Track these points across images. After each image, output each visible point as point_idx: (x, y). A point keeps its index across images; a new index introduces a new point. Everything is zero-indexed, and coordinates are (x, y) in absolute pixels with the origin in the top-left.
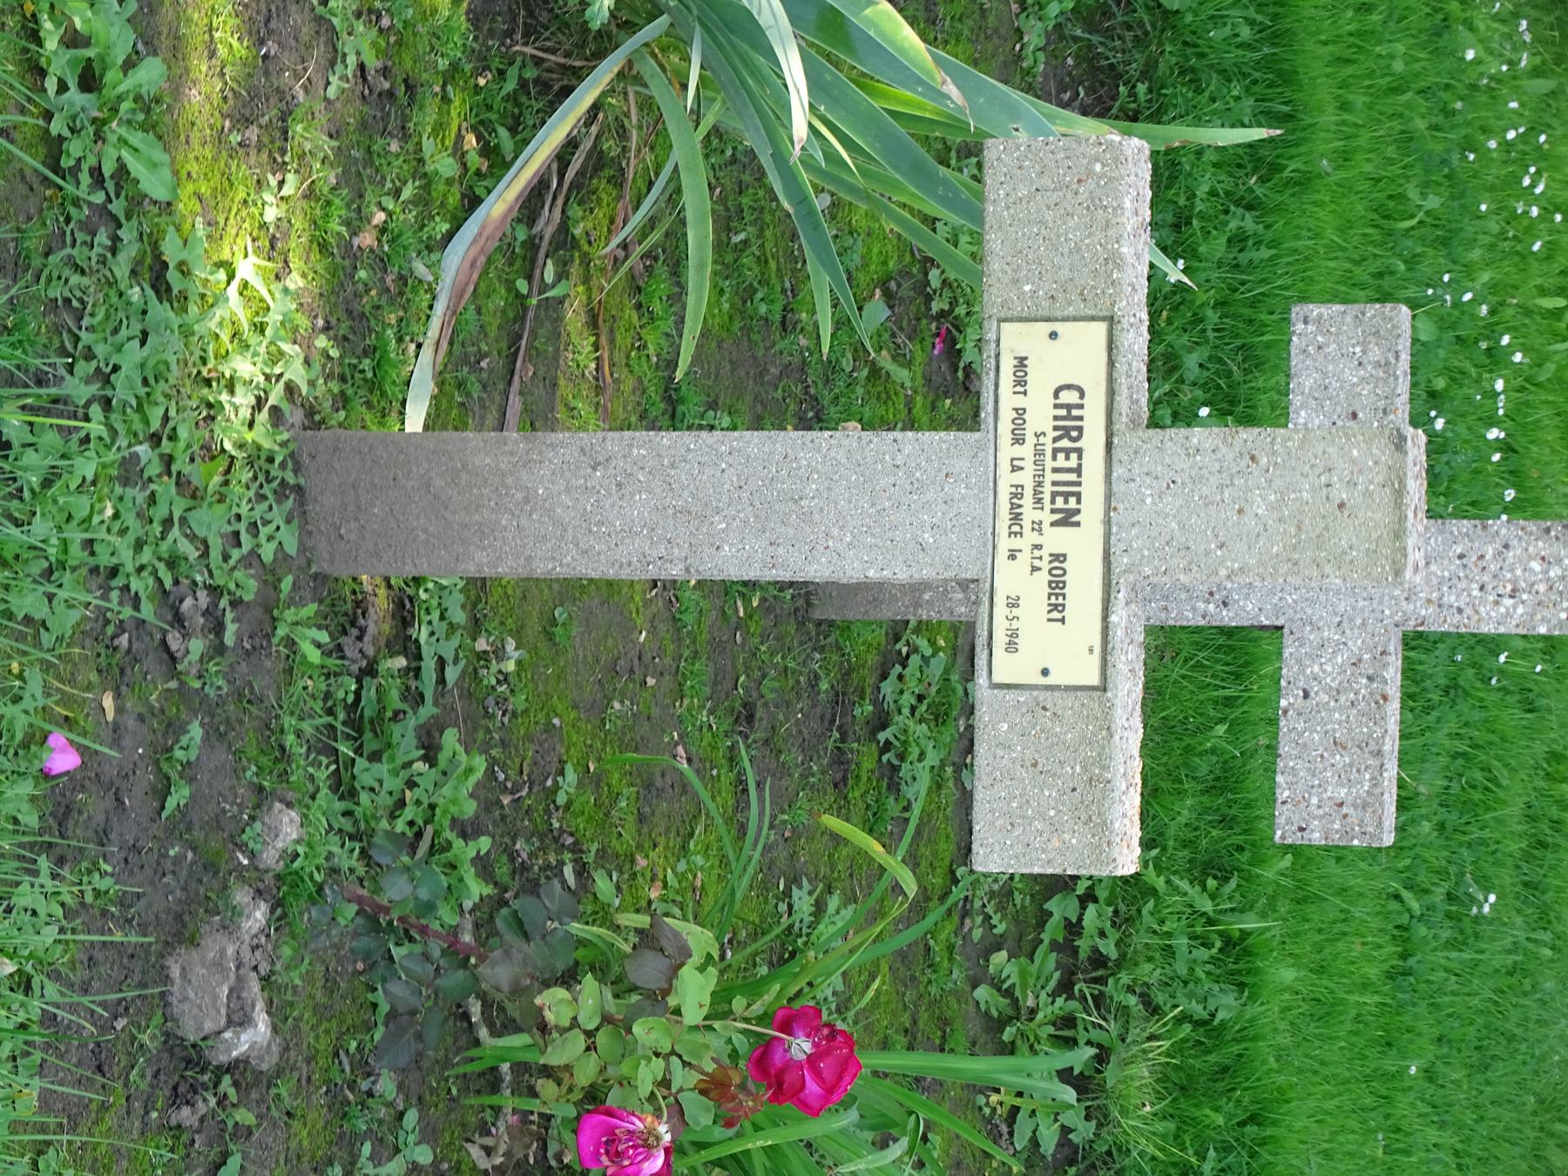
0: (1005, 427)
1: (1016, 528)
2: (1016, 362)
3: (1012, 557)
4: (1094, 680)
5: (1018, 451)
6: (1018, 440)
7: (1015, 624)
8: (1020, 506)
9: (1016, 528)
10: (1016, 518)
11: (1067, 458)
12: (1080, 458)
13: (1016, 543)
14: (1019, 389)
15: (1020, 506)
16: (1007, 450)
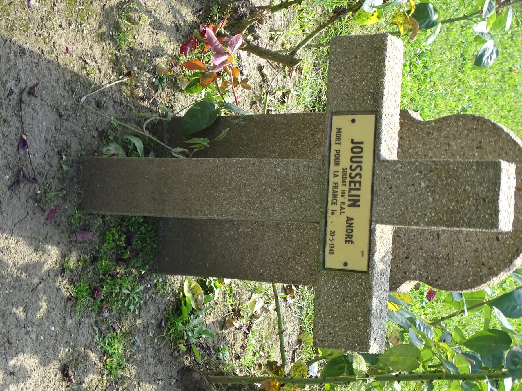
0: (333, 158)
1: (334, 201)
2: (337, 131)
3: (333, 213)
4: (365, 269)
5: (336, 168)
6: (337, 164)
7: (333, 242)
8: (337, 192)
9: (334, 201)
10: (335, 197)
11: (355, 185)
12: (360, 185)
13: (334, 207)
14: (338, 142)
15: (337, 192)
16: (333, 168)
